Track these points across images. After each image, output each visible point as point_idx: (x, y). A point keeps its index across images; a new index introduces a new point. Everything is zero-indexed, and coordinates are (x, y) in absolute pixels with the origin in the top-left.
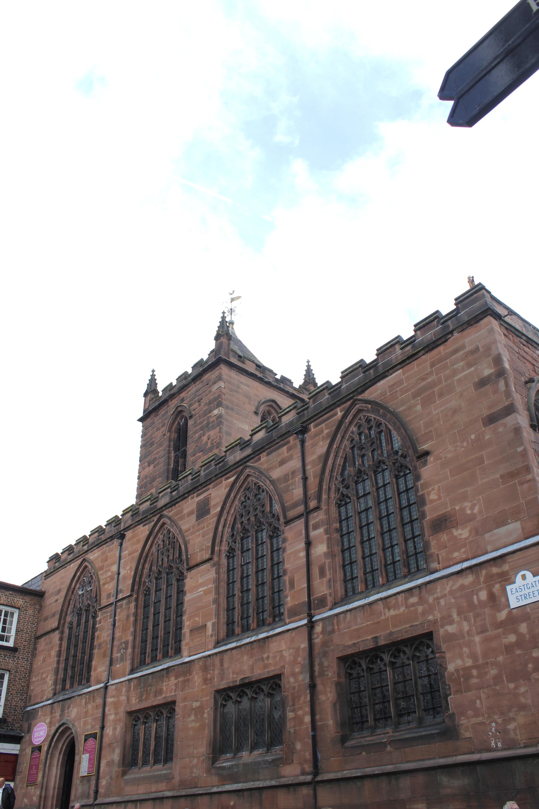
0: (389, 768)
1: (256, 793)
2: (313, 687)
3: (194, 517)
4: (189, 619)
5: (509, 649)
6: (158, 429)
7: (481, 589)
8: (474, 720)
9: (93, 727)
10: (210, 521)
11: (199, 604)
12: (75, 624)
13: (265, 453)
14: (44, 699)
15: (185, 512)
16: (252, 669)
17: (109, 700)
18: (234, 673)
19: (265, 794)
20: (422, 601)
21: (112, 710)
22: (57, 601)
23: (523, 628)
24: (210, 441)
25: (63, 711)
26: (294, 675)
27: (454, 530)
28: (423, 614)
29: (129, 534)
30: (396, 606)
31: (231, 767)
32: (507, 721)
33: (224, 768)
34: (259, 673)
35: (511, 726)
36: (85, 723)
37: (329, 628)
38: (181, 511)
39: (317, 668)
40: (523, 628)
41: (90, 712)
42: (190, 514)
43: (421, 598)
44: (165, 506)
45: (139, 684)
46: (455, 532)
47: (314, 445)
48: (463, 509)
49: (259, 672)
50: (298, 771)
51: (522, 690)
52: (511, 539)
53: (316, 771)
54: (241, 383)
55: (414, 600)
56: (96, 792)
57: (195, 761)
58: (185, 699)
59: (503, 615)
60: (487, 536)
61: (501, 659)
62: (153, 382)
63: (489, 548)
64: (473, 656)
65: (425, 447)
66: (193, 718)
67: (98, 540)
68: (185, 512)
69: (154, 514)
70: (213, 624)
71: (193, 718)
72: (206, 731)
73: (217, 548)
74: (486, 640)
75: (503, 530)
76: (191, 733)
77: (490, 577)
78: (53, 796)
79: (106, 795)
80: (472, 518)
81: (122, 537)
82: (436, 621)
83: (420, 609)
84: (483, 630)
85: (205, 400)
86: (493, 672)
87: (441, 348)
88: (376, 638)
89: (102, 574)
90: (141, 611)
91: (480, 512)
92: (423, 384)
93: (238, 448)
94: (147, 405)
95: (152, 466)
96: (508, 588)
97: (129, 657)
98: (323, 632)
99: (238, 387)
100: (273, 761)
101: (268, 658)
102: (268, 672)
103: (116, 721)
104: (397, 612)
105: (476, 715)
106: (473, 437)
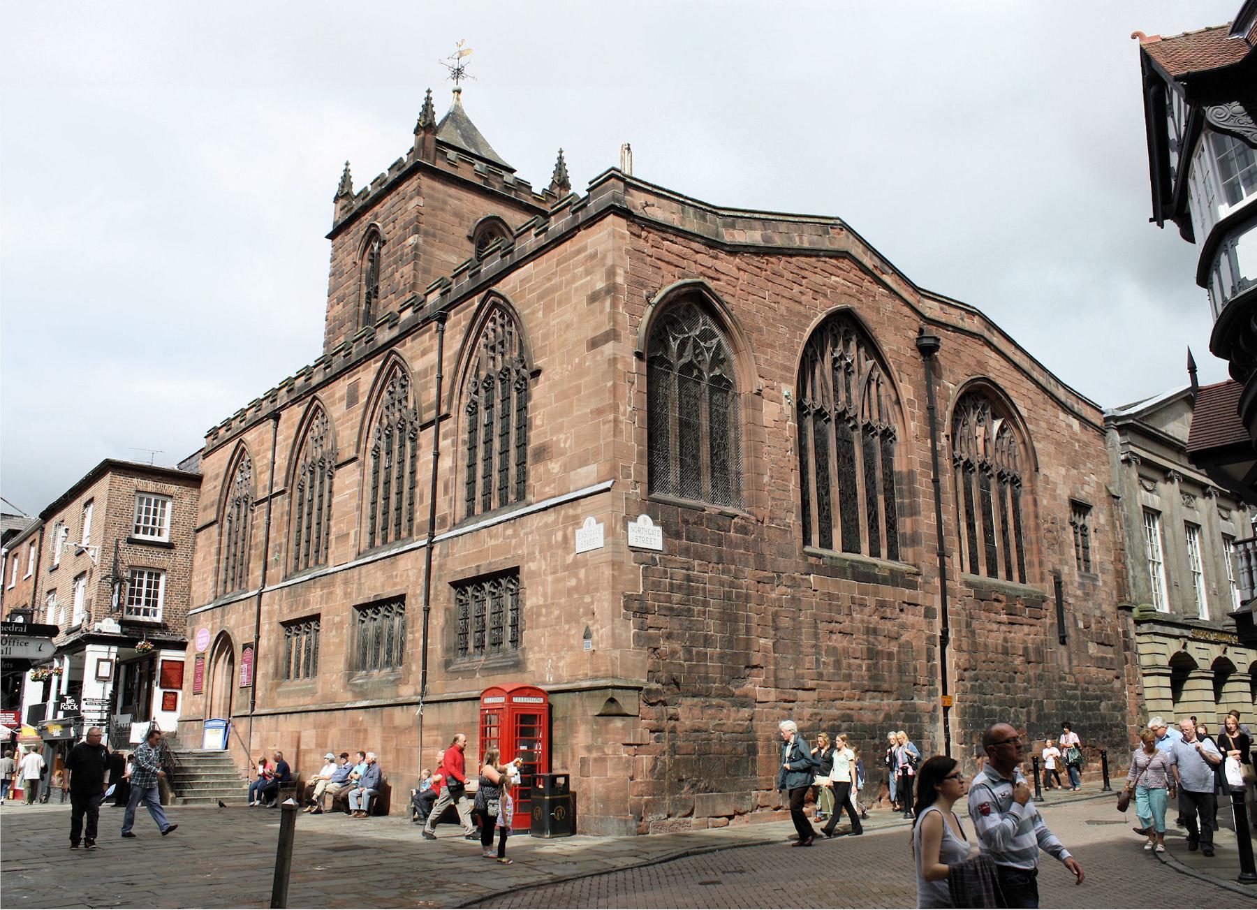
2: (427, 610)
3: (345, 403)
5: (570, 591)
6: (349, 254)
7: (559, 529)
9: (250, 636)
10: (358, 409)
11: (346, 509)
12: (234, 519)
13: (410, 338)
14: (206, 602)
15: (337, 396)
16: (383, 586)
17: (264, 608)
20: (515, 535)
22: (215, 487)
24: (402, 280)
25: (223, 616)
26: (415, 596)
27: (549, 462)
29: (284, 414)
31: (362, 685)
32: (560, 658)
33: (356, 685)
35: (561, 664)
36: (243, 630)
37: (445, 552)
38: (332, 395)
39: (432, 592)
40: (582, 573)
41: (247, 621)
42: (341, 399)
43: (514, 531)
44: (318, 385)
45: (288, 594)
47: (452, 338)
48: (558, 441)
49: (389, 590)
51: (573, 632)
52: (588, 482)
53: (423, 693)
54: (450, 196)
55: (510, 532)
56: (253, 704)
58: (328, 613)
59: (570, 559)
60: (572, 473)
61: (563, 600)
62: (346, 180)
63: (571, 488)
64: (545, 595)
65: (538, 363)
66: (334, 633)
67: (255, 416)
68: (337, 396)
69: (308, 393)
70: (356, 533)
71: (334, 633)
72: (345, 648)
73: (363, 446)
74: (556, 581)
75: (583, 471)
76: (332, 648)
78: (220, 705)
79: (262, 707)
80: (562, 453)
81: (275, 416)
82: (523, 557)
83: (513, 542)
85: (400, 223)
86: (556, 613)
88: (478, 566)
89: (259, 461)
90: (295, 509)
91: (571, 445)
92: (548, 285)
93: (387, 325)
94: (338, 215)
95: (341, 304)
96: (577, 532)
97: (282, 562)
98: (440, 555)
99: (445, 203)
100: (395, 680)
103: (270, 631)
105: (540, 652)
106: (577, 360)
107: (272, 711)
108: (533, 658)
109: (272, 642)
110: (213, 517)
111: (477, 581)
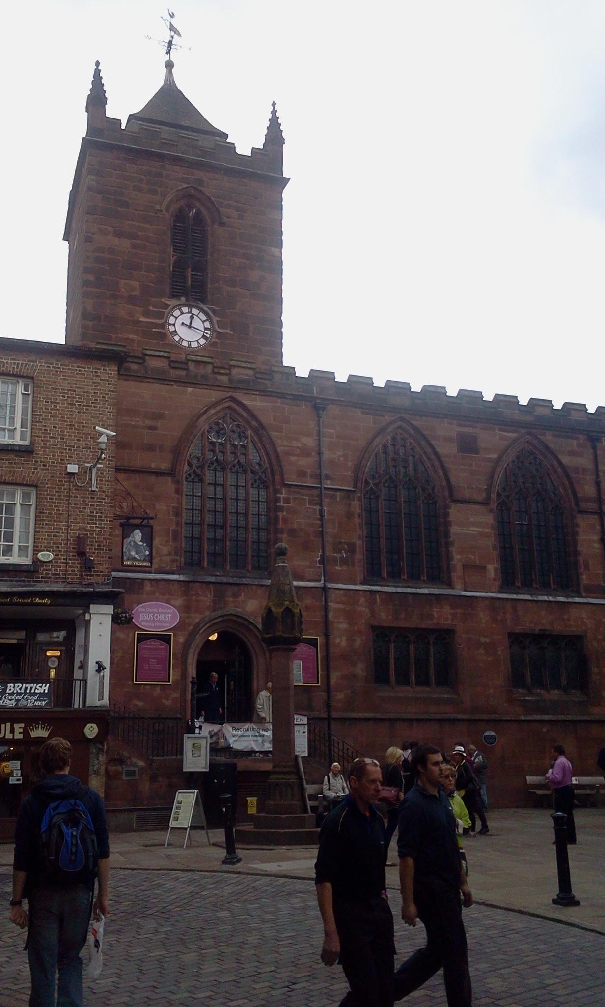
21: (342, 618)
34: (558, 628)
57: (491, 691)
66: (482, 651)
107: (378, 716)
109: (358, 642)
110: (165, 466)
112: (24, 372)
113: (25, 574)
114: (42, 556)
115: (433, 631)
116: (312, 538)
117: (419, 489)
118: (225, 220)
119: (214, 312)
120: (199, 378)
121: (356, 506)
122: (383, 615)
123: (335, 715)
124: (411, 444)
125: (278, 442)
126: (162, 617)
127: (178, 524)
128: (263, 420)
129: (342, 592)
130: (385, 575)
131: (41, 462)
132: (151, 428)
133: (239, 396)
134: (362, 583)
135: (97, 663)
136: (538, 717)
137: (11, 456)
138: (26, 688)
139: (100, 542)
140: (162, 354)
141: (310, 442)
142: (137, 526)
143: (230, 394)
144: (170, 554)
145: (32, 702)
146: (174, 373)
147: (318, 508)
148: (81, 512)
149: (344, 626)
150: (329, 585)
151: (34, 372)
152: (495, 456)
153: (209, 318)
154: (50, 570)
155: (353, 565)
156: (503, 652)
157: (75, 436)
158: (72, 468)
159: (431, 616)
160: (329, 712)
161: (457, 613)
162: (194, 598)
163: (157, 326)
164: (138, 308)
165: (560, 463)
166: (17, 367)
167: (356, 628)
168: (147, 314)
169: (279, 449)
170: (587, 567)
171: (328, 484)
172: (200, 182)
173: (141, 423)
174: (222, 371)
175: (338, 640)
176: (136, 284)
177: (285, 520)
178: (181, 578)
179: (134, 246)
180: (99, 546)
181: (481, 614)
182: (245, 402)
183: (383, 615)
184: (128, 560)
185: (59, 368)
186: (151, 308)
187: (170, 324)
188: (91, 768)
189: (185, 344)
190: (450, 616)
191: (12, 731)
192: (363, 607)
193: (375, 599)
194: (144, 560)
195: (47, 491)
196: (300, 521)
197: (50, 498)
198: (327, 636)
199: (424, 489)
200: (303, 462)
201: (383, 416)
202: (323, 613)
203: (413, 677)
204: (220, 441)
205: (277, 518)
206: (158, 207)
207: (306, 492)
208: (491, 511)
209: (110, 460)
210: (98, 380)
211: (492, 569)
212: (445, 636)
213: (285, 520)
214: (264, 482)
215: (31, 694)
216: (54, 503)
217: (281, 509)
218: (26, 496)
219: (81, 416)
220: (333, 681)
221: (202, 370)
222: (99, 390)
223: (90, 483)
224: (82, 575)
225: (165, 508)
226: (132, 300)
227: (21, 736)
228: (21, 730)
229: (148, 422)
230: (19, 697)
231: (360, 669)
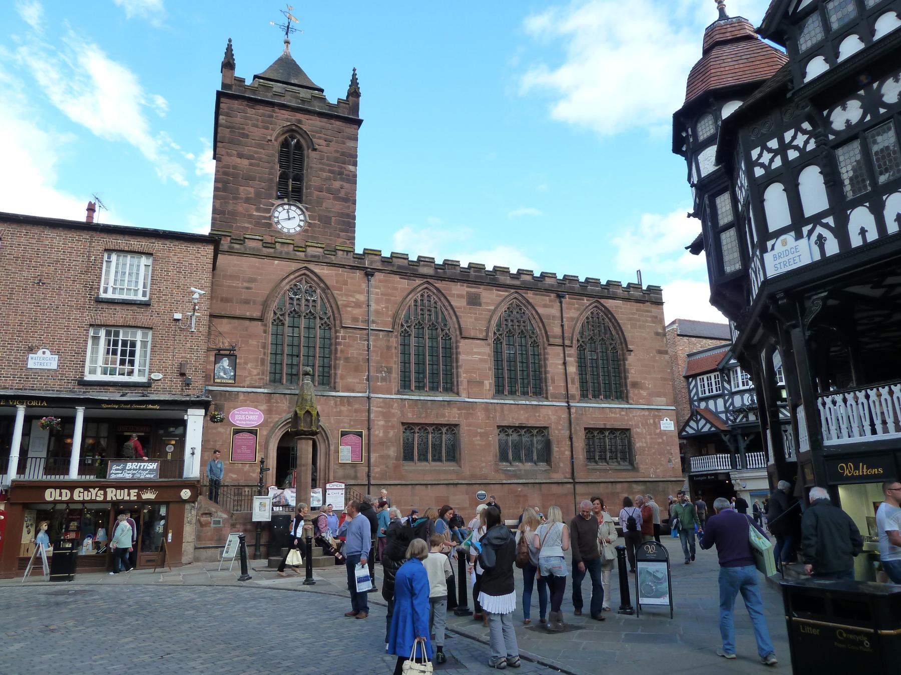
0: (612, 480)
1: (538, 486)
2: (571, 438)
4: (466, 372)
5: (659, 444)
8: (646, 467)
14: (247, 383)
18: (513, 418)
19: (543, 486)
23: (665, 438)
28: (627, 420)
30: (615, 413)
31: (513, 471)
32: (657, 468)
34: (531, 423)
35: (658, 470)
46: (642, 392)
49: (533, 422)
50: (562, 476)
51: (662, 459)
52: (662, 404)
55: (623, 413)
57: (484, 464)
59: (658, 431)
61: (656, 446)
64: (646, 443)
66: (478, 438)
74: (651, 438)
75: (659, 399)
76: (478, 447)
77: (655, 416)
80: (648, 388)
83: (626, 418)
84: (650, 434)
87: (642, 305)
100: (546, 470)
101: (539, 416)
102: (540, 424)
104: (615, 416)
107: (404, 482)
108: (642, 468)
109: (391, 434)
110: (256, 314)
111: (602, 431)
112: (146, 250)
113: (142, 388)
114: (153, 376)
115: (445, 425)
116: (361, 363)
117: (439, 330)
118: (317, 147)
119: (307, 208)
120: (283, 254)
121: (395, 341)
122: (410, 415)
123: (372, 482)
124: (434, 299)
125: (339, 298)
126: (251, 417)
127: (264, 354)
128: (329, 283)
129: (381, 400)
130: (413, 388)
131: (156, 311)
132: (248, 288)
133: (311, 266)
134: (395, 394)
135: (192, 448)
136: (516, 481)
137: (135, 308)
138: (141, 466)
139: (197, 366)
140: (257, 237)
141: (362, 298)
142: (225, 356)
143: (305, 265)
144: (258, 374)
145: (144, 475)
146: (266, 251)
147: (366, 343)
148: (183, 346)
149: (382, 423)
150: (372, 395)
151: (153, 250)
152: (493, 308)
153: (303, 213)
154: (160, 386)
155: (390, 382)
156: (494, 438)
157: (181, 294)
158: (178, 316)
159: (443, 416)
160: (369, 480)
161: (462, 413)
162: (275, 404)
163: (265, 218)
164: (252, 206)
165: (537, 312)
166: (141, 246)
167: (390, 424)
168: (258, 210)
169: (339, 303)
170: (553, 381)
171: (374, 327)
172: (300, 121)
173: (240, 285)
174: (300, 249)
175: (377, 432)
176: (251, 190)
177: (342, 351)
178: (266, 391)
179: (251, 165)
180: (195, 369)
181: (479, 414)
182: (316, 271)
183: (410, 415)
184: (218, 378)
185: (171, 247)
186: (262, 206)
187: (275, 217)
188: (185, 519)
189: (285, 230)
190: (457, 415)
191: (129, 495)
192: (396, 410)
193: (405, 405)
194: (230, 379)
195: (159, 331)
196: (353, 352)
197: (161, 337)
198: (369, 429)
199: (442, 330)
200: (356, 312)
201: (415, 280)
202: (367, 414)
203: (430, 457)
204: (297, 297)
205: (336, 350)
206: (269, 138)
207: (358, 331)
208: (489, 345)
209: (205, 310)
210: (199, 255)
211: (489, 383)
212: (453, 428)
213: (342, 351)
214: (329, 325)
215: (143, 470)
216: (165, 340)
217: (340, 344)
218: (145, 335)
219: (186, 280)
220: (372, 460)
221: (286, 249)
222: (200, 262)
223: (190, 326)
224: (182, 389)
225: (256, 343)
226: (248, 200)
227: (135, 498)
228: (136, 494)
229: (245, 284)
230: (135, 472)
231: (392, 452)
